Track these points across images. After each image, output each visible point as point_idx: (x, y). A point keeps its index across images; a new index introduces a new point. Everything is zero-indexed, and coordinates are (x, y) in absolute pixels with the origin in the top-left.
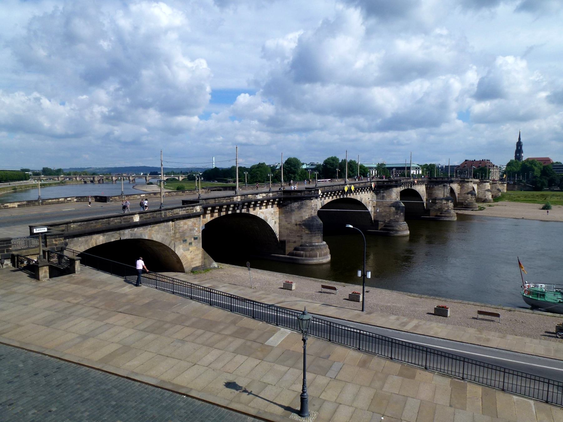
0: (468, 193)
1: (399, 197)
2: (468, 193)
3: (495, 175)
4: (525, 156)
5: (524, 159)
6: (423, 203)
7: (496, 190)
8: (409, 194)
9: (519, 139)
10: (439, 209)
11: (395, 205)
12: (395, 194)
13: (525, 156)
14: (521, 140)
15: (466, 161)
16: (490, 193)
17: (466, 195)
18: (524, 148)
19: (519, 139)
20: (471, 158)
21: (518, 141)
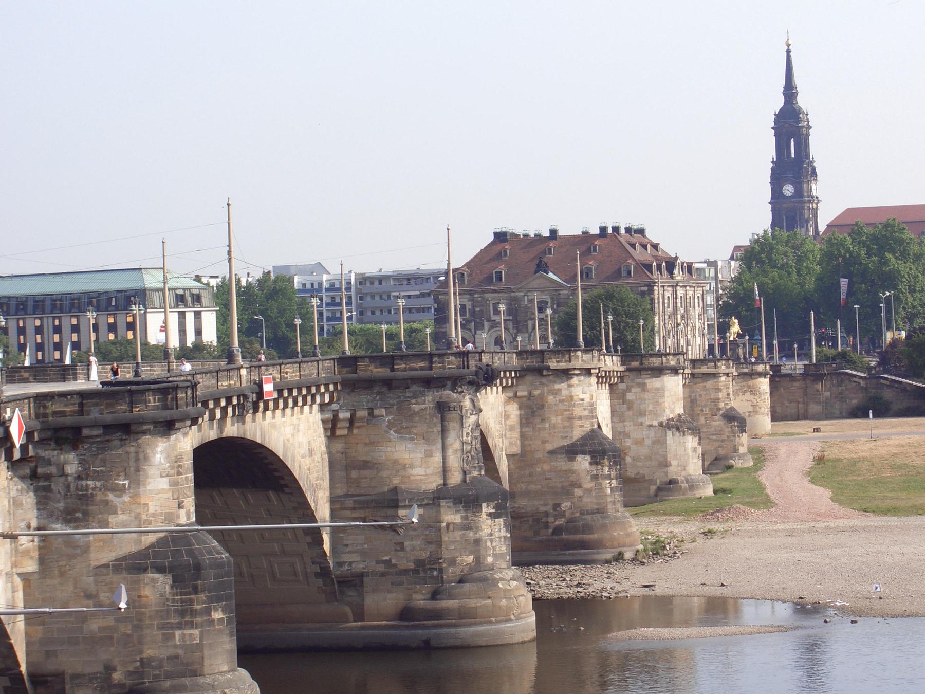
0: (572, 451)
1: (190, 503)
2: (572, 451)
3: (686, 322)
4: (834, 197)
5: (825, 216)
6: (316, 534)
7: (718, 422)
8: (236, 472)
9: (790, 91)
10: (420, 563)
11: (170, 557)
12: (160, 487)
13: (834, 197)
14: (802, 101)
15: (500, 237)
16: (691, 442)
17: (562, 463)
18: (819, 149)
19: (790, 91)
20: (530, 223)
21: (779, 102)
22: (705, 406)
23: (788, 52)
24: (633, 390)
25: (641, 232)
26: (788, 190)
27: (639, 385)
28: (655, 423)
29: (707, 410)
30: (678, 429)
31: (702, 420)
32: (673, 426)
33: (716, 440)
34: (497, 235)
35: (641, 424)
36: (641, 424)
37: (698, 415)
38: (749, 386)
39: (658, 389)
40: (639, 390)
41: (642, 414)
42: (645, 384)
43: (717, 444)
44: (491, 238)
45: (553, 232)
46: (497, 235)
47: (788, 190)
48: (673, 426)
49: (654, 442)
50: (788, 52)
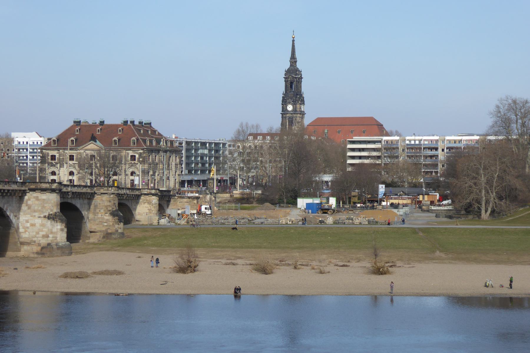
5: (308, 120)
9: (293, 59)
14: (299, 65)
18: (306, 88)
19: (293, 59)
20: (91, 118)
21: (287, 66)
22: (102, 209)
23: (293, 41)
24: (31, 200)
26: (290, 108)
28: (42, 216)
29: (102, 211)
30: (54, 219)
31: (100, 215)
33: (106, 226)
34: (75, 122)
35: (35, 216)
37: (98, 213)
38: (147, 200)
43: (107, 228)
44: (72, 124)
45: (102, 123)
46: (75, 122)
47: (290, 108)
48: (51, 218)
50: (293, 41)
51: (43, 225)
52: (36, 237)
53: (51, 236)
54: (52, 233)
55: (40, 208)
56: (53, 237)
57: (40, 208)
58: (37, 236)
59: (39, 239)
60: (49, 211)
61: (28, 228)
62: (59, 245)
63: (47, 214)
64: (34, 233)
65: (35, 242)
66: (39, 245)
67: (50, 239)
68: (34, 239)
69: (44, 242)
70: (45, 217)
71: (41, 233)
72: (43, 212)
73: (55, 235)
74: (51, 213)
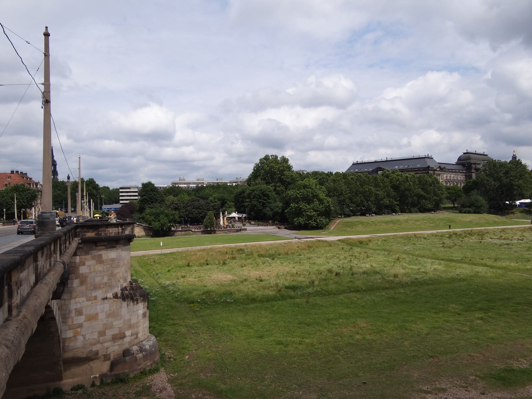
24: (87, 263)
25: (26, 174)
27: (93, 258)
28: (110, 295)
30: (132, 299)
32: (127, 297)
35: (96, 298)
36: (96, 298)
39: (113, 260)
40: (93, 262)
41: (96, 288)
42: (100, 256)
48: (127, 297)
49: (108, 316)
51: (112, 315)
52: (98, 342)
53: (128, 333)
54: (130, 327)
55: (105, 279)
56: (132, 335)
57: (105, 279)
58: (101, 339)
59: (106, 345)
60: (122, 281)
61: (81, 326)
62: (145, 350)
63: (118, 290)
64: (96, 336)
65: (97, 353)
66: (106, 357)
67: (127, 339)
68: (95, 348)
69: (115, 349)
70: (116, 296)
71: (109, 333)
72: (111, 287)
73: (135, 330)
74: (125, 285)
